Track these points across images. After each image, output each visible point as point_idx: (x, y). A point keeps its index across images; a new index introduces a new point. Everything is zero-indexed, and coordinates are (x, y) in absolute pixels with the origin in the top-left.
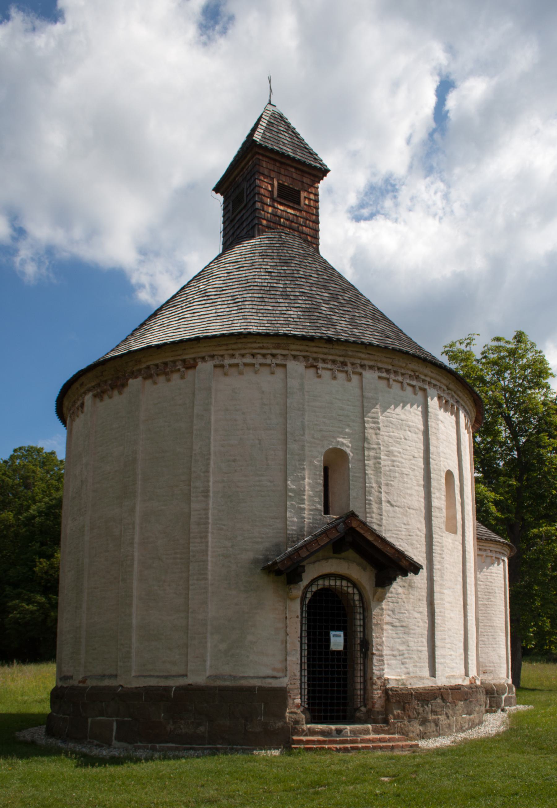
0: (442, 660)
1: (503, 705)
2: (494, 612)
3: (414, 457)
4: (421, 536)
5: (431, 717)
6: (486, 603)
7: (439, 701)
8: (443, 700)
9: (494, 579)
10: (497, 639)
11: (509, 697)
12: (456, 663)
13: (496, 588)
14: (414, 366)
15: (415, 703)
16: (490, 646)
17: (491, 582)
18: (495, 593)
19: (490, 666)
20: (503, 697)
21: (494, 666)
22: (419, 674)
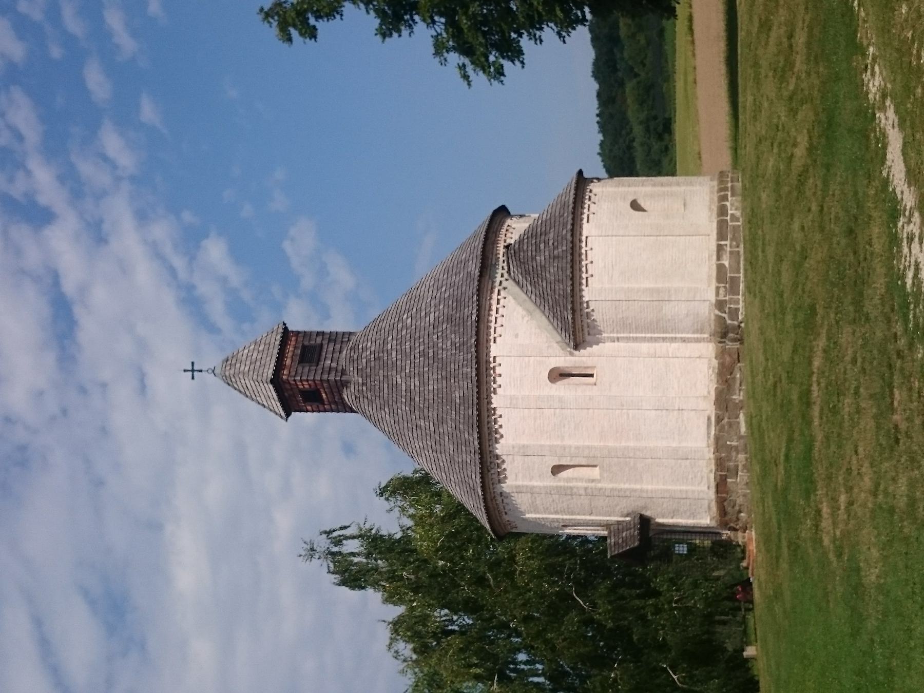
0: (696, 493)
2: (643, 320)
3: (553, 501)
4: (609, 500)
5: (737, 508)
7: (725, 504)
8: (725, 500)
9: (609, 318)
10: (670, 317)
12: (698, 472)
13: (618, 317)
14: (490, 505)
15: (727, 518)
16: (676, 325)
17: (613, 322)
18: (623, 318)
19: (697, 326)
20: (729, 322)
21: (697, 322)
22: (706, 505)
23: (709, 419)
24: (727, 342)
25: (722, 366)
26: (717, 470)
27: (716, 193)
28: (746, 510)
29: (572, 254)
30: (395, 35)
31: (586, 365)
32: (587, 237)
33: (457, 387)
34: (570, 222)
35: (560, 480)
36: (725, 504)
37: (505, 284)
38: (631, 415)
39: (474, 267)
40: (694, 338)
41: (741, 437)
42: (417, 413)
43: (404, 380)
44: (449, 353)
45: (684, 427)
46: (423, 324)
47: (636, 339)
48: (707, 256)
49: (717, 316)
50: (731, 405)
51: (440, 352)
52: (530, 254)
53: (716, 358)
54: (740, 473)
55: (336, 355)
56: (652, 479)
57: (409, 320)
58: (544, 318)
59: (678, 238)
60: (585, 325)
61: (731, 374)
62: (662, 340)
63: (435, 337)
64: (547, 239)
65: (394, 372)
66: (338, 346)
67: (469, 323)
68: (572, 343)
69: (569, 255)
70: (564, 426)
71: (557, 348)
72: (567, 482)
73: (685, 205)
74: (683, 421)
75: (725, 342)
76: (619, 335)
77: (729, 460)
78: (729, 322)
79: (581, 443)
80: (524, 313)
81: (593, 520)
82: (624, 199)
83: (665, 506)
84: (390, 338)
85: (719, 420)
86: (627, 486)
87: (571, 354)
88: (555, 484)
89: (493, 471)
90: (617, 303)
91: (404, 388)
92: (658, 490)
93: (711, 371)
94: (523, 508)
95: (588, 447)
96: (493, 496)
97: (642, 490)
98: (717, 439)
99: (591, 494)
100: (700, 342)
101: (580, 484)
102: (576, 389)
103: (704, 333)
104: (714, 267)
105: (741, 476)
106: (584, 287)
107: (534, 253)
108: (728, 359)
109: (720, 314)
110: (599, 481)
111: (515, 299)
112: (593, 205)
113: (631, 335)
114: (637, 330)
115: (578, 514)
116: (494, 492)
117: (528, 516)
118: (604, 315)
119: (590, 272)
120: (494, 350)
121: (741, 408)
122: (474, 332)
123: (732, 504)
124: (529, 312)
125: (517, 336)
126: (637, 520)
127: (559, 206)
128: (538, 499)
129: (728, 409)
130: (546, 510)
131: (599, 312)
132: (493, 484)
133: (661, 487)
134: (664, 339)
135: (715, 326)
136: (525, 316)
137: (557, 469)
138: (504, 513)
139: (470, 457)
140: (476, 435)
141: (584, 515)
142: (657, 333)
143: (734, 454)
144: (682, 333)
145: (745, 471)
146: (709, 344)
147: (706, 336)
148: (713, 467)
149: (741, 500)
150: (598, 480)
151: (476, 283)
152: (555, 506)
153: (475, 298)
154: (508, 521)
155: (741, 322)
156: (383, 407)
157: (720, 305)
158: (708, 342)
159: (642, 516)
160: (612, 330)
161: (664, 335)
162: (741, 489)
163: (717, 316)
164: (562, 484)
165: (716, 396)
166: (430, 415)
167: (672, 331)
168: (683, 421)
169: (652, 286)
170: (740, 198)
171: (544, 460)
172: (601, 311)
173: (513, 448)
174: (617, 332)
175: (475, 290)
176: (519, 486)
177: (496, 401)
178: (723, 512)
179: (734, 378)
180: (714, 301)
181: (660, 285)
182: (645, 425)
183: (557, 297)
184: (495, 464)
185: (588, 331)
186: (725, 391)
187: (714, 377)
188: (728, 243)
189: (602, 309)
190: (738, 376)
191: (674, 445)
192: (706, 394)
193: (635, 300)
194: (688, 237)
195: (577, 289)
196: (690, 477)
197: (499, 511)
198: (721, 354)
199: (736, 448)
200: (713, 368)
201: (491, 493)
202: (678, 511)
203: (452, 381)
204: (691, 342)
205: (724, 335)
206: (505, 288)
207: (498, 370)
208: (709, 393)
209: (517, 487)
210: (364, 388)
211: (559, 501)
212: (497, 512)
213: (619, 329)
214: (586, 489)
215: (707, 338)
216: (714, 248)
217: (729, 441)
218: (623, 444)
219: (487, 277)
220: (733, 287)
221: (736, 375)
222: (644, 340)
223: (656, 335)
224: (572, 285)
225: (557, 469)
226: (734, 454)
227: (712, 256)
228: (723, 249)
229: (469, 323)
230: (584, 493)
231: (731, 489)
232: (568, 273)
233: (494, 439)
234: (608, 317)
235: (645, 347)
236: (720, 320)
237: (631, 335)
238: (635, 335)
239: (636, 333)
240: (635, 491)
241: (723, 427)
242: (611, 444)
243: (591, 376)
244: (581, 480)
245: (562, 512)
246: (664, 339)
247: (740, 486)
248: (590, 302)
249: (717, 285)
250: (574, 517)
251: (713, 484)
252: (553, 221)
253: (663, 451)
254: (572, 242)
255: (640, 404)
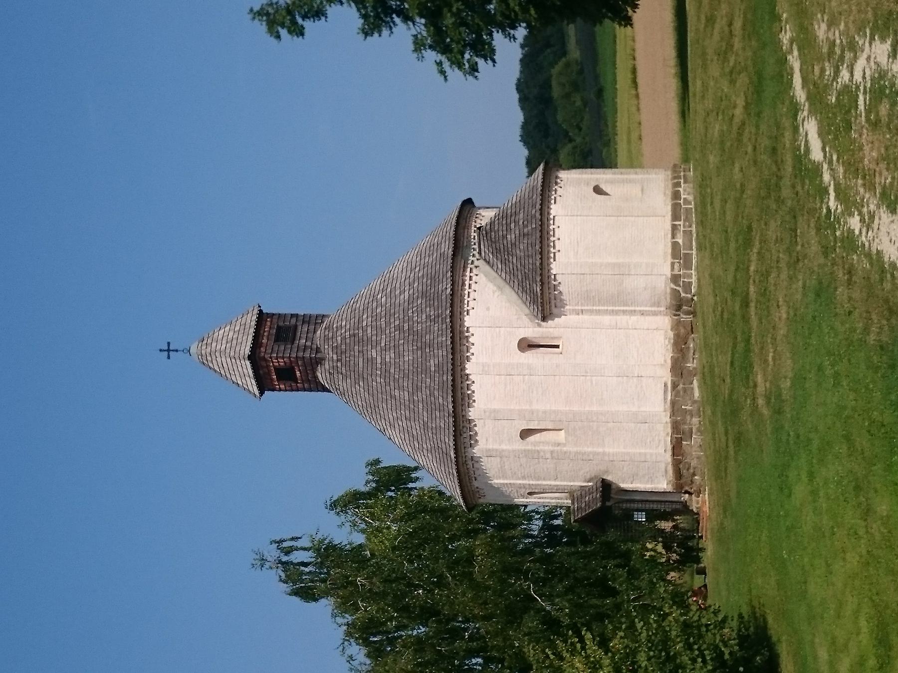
0: (654, 457)
1: (689, 296)
3: (521, 465)
6: (597, 299)
7: (681, 466)
11: (683, 286)
12: (656, 436)
14: (462, 469)
17: (578, 295)
18: (587, 291)
20: (683, 295)
21: (655, 295)
22: (663, 470)
23: (666, 385)
24: (681, 314)
25: (677, 336)
26: (673, 433)
27: (670, 181)
28: (699, 472)
29: (541, 231)
30: (376, 35)
31: (552, 336)
32: (554, 217)
33: (432, 356)
34: (539, 202)
35: (528, 444)
36: (681, 466)
37: (476, 263)
38: (594, 382)
39: (447, 248)
40: (652, 311)
41: (695, 402)
42: (392, 383)
43: (379, 353)
44: (424, 326)
45: (643, 392)
46: (397, 301)
47: (598, 312)
48: (663, 234)
49: (672, 289)
50: (685, 372)
51: (415, 325)
52: (501, 233)
53: (672, 330)
54: (694, 436)
55: (310, 335)
56: (614, 442)
57: (384, 299)
58: (513, 292)
59: (637, 218)
60: (553, 298)
61: (686, 343)
62: (622, 314)
63: (410, 311)
64: (517, 219)
65: (370, 347)
66: (312, 327)
67: (444, 297)
68: (540, 315)
69: (538, 231)
70: (532, 392)
71: (526, 320)
72: (535, 446)
73: (642, 190)
74: (642, 387)
75: (679, 315)
76: (583, 308)
77: (685, 423)
78: (683, 295)
79: (548, 408)
80: (495, 288)
81: (558, 485)
82: (588, 184)
83: (625, 469)
84: (365, 316)
85: (675, 386)
86: (590, 449)
87: (539, 325)
88: (523, 448)
89: (465, 435)
90: (582, 276)
91: (379, 361)
92: (619, 453)
93: (667, 342)
94: (490, 474)
95: (554, 411)
96: (464, 459)
97: (604, 454)
98: (673, 403)
99: (557, 457)
100: (657, 315)
101: (546, 448)
102: (544, 358)
103: (661, 307)
104: (670, 244)
105: (695, 438)
106: (552, 260)
107: (505, 233)
108: (682, 331)
109: (675, 287)
110: (565, 445)
111: (486, 276)
112: (560, 188)
113: (594, 308)
114: (600, 303)
115: (544, 479)
116: (466, 456)
117: (496, 481)
118: (570, 288)
119: (557, 248)
120: (468, 321)
121: (695, 375)
122: (449, 305)
123: (687, 466)
124: (500, 288)
125: (488, 309)
126: (599, 484)
127: (527, 190)
128: (506, 464)
129: (683, 376)
130: (514, 475)
131: (565, 285)
132: (465, 447)
133: (622, 450)
134: (624, 312)
135: (671, 299)
136: (496, 291)
137: (526, 434)
138: (474, 479)
139: (445, 423)
140: (450, 399)
141: (550, 480)
142: (618, 306)
143: (688, 417)
144: (641, 306)
145: (699, 434)
146: (665, 317)
147: (662, 309)
148: (669, 431)
149: (696, 462)
150: (563, 444)
151: (450, 261)
152: (523, 471)
153: (449, 274)
154: (477, 488)
155: (694, 296)
156: (357, 381)
157: (675, 279)
158: (664, 315)
159: (603, 480)
160: (577, 302)
161: (625, 308)
162: (695, 451)
163: (672, 289)
164: (529, 447)
165: (672, 363)
166: (405, 384)
167: (632, 304)
168: (642, 387)
169: (614, 261)
170: (691, 185)
171: (514, 425)
172: (567, 284)
173: (485, 412)
174: (582, 305)
175: (449, 267)
176: (489, 450)
177: (470, 368)
178: (678, 474)
179: (689, 348)
180: (669, 276)
181: (621, 260)
182: (607, 391)
183: (527, 271)
184: (467, 428)
185: (555, 303)
186: (681, 359)
187: (670, 347)
188: (681, 223)
189: (568, 282)
190: (692, 346)
191: (634, 409)
192: (663, 362)
193: (597, 274)
194: (646, 218)
195: (545, 264)
196: (648, 441)
197: (469, 476)
198: (677, 326)
199: (691, 411)
200: (669, 338)
201: (462, 457)
202: (637, 475)
203: (428, 350)
204: (649, 315)
205: (678, 308)
206: (476, 267)
207: (471, 340)
208: (665, 361)
209: (488, 450)
210: (339, 364)
211: (526, 465)
212: (467, 477)
213: (583, 302)
214: (552, 452)
215: (664, 311)
216: (669, 227)
217: (684, 406)
218: (587, 409)
219: (460, 257)
220: (687, 265)
221: (690, 344)
222: (606, 312)
223: (617, 308)
224: (541, 259)
225: (526, 434)
226: (688, 417)
227: (667, 234)
228: (677, 229)
229: (444, 297)
230: (550, 457)
231: (686, 451)
232: (538, 247)
233: (467, 404)
234: (573, 290)
235: (607, 319)
236: (675, 293)
237: (594, 308)
238: (598, 308)
239: (599, 306)
240: (598, 454)
241: (678, 392)
242: (576, 408)
243: (557, 347)
244: (548, 443)
245: (530, 477)
246: (624, 312)
247: (694, 449)
248: (557, 275)
249: (672, 260)
250: (540, 482)
251: (669, 447)
252: (522, 202)
253: (623, 415)
254: (541, 220)
255: (603, 372)
